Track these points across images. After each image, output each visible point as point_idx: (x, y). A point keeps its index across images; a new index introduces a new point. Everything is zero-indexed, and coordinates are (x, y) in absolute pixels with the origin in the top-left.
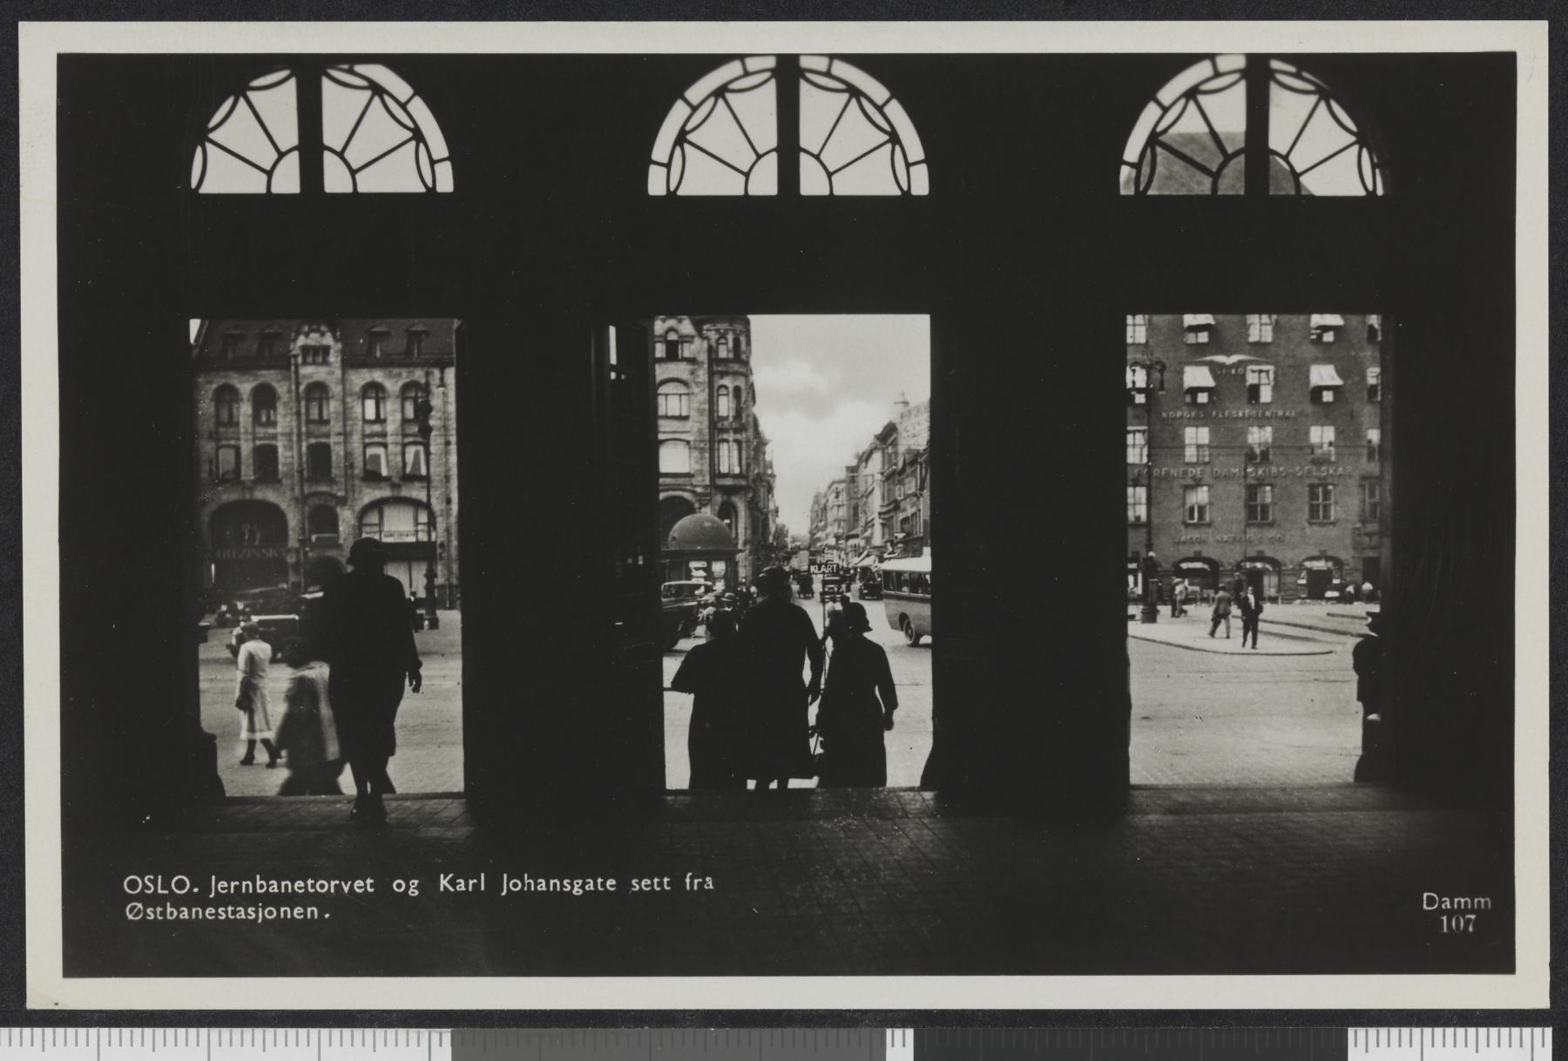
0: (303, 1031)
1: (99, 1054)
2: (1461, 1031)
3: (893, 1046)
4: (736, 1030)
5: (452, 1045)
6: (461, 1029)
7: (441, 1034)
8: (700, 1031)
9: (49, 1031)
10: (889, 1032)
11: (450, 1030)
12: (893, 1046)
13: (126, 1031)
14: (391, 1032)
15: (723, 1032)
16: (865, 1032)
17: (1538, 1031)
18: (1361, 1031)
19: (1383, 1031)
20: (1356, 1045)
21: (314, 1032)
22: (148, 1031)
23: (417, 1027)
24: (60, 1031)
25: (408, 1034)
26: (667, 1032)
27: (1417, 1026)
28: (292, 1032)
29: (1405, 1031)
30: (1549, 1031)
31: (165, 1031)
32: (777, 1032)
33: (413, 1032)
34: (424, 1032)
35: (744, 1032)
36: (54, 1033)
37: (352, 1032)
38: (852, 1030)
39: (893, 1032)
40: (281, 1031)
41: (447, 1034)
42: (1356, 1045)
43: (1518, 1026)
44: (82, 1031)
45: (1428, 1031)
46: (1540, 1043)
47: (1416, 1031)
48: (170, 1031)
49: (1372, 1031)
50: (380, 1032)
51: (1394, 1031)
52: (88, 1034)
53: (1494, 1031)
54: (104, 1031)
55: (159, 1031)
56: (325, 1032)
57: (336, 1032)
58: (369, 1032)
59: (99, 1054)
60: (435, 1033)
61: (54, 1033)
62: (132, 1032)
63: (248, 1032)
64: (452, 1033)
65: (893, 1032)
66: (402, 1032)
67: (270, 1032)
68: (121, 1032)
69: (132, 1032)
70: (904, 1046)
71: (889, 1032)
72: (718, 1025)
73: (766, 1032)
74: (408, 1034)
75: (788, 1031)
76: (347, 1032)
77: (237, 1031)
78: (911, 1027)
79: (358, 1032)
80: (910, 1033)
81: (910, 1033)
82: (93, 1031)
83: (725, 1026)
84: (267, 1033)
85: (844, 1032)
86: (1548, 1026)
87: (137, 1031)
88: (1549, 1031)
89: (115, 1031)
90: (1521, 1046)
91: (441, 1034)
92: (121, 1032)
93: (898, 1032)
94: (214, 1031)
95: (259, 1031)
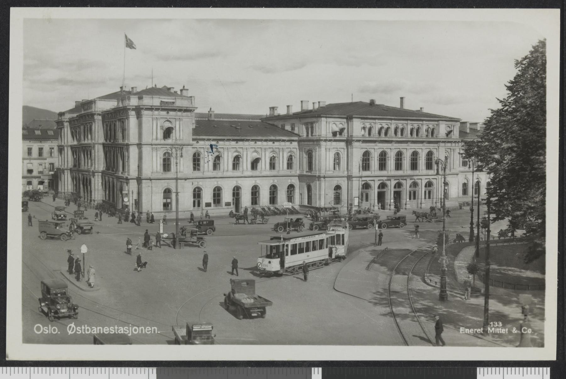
0: (103, 368)
1: (30, 377)
2: (517, 369)
3: (314, 374)
4: (258, 368)
5: (157, 373)
6: (160, 368)
7: (153, 369)
8: (245, 369)
9: (12, 368)
10: (313, 369)
11: (156, 368)
12: (314, 374)
13: (40, 368)
14: (135, 369)
15: (254, 368)
16: (304, 369)
17: (545, 368)
18: (482, 369)
19: (490, 369)
20: (480, 374)
21: (107, 368)
22: (48, 368)
23: (144, 367)
24: (16, 368)
25: (141, 369)
26: (233, 369)
27: (502, 367)
28: (99, 368)
29: (497, 368)
30: (549, 369)
31: (54, 368)
32: (273, 369)
33: (143, 369)
34: (147, 368)
35: (261, 369)
36: (14, 369)
37: (121, 369)
38: (300, 368)
39: (314, 369)
40: (95, 368)
41: (155, 369)
42: (480, 374)
43: (545, 367)
44: (24, 368)
45: (505, 368)
46: (546, 372)
47: (501, 369)
48: (56, 368)
49: (486, 369)
50: (131, 369)
51: (494, 369)
52: (26, 369)
53: (529, 368)
54: (32, 368)
55: (52, 368)
56: (111, 368)
57: (115, 368)
58: (127, 369)
59: (30, 377)
60: (151, 369)
61: (14, 369)
62: (42, 368)
63: (83, 368)
64: (157, 369)
65: (314, 369)
66: (139, 369)
67: (91, 368)
68: (38, 369)
69: (42, 368)
70: (318, 374)
71: (313, 369)
72: (252, 366)
73: (269, 369)
74: (141, 369)
75: (277, 369)
76: (119, 368)
77: (80, 368)
78: (320, 367)
79: (123, 369)
80: (320, 369)
81: (320, 369)
82: (28, 368)
83: (254, 367)
84: (481, 369)
85: (297, 369)
86: (549, 367)
87: (44, 368)
88: (549, 369)
89: (36, 368)
90: (539, 374)
91: (153, 369)
92: (38, 369)
93: (316, 369)
94: (72, 368)
95: (87, 368)
